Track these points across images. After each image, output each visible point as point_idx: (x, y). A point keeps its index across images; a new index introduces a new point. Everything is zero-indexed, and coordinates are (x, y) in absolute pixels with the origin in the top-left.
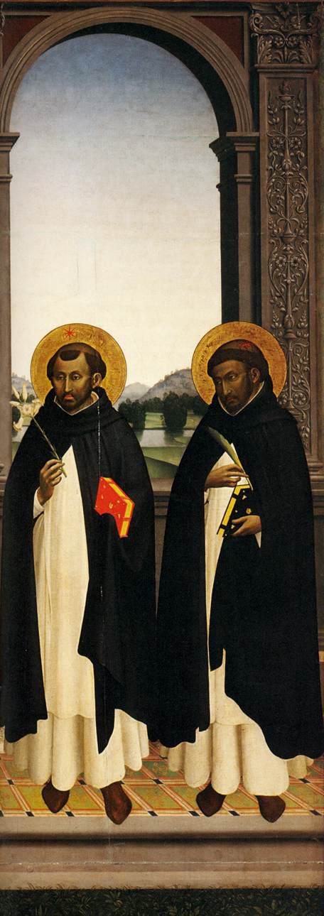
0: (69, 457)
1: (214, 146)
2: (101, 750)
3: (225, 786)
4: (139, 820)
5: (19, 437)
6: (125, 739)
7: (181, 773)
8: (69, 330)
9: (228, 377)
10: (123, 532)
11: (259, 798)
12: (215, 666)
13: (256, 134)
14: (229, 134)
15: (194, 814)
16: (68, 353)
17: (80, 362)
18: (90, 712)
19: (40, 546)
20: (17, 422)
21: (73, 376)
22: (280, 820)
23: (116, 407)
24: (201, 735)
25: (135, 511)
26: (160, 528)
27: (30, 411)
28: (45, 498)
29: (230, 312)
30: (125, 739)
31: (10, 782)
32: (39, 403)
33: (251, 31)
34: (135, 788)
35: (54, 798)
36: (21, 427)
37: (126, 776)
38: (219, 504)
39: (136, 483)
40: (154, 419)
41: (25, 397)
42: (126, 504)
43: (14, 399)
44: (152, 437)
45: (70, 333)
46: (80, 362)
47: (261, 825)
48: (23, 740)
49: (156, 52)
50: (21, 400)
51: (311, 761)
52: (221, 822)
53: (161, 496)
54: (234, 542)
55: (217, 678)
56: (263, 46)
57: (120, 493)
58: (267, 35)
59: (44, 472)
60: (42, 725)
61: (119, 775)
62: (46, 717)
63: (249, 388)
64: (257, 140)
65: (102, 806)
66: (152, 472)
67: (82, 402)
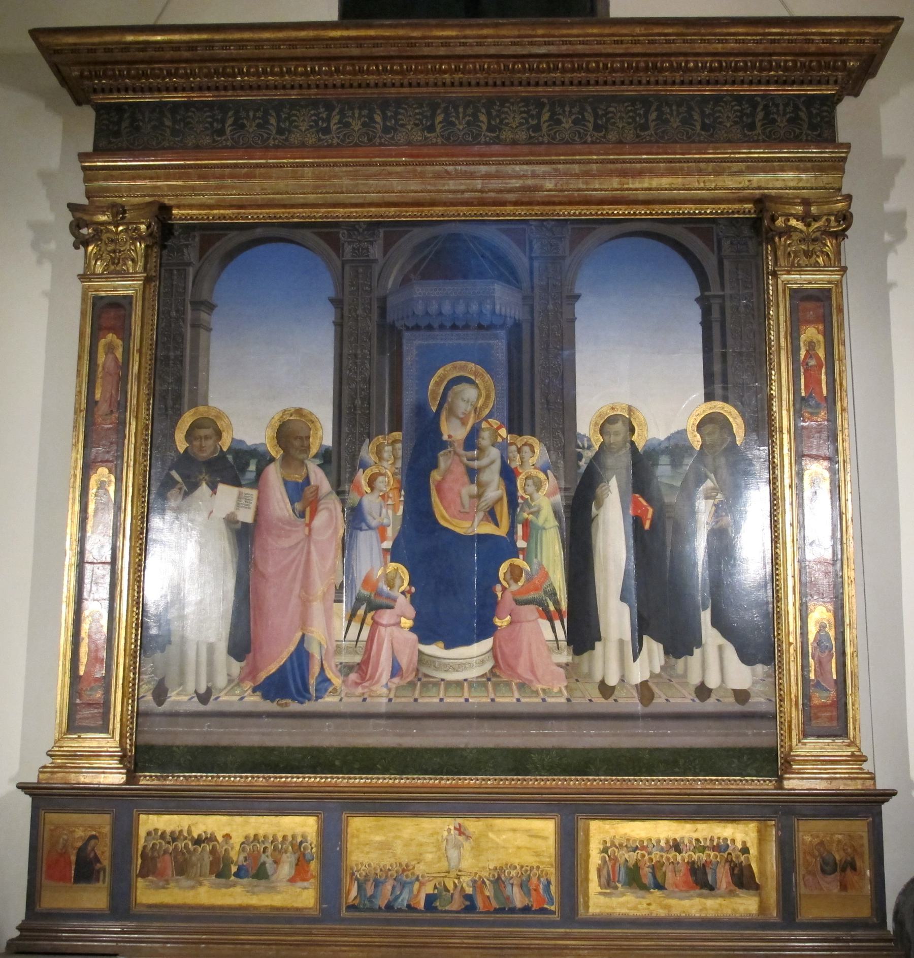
1: (697, 300)
2: (635, 660)
3: (713, 682)
4: (660, 703)
7: (685, 675)
10: (647, 526)
12: (704, 609)
13: (722, 293)
14: (707, 293)
15: (693, 700)
16: (611, 420)
17: (619, 426)
18: (627, 636)
19: (596, 535)
20: (580, 460)
22: (747, 705)
24: (697, 652)
25: (654, 513)
27: (588, 455)
28: (599, 507)
29: (709, 397)
31: (577, 680)
33: (718, 235)
34: (657, 684)
35: (605, 690)
36: (583, 464)
37: (651, 677)
41: (586, 446)
43: (578, 447)
45: (613, 409)
46: (619, 426)
47: (738, 708)
48: (586, 655)
49: (661, 246)
50: (583, 448)
51: (766, 668)
52: (710, 705)
56: (726, 244)
57: (645, 503)
58: (727, 237)
59: (599, 491)
60: (598, 645)
61: (647, 676)
62: (599, 639)
64: (722, 297)
65: (635, 694)
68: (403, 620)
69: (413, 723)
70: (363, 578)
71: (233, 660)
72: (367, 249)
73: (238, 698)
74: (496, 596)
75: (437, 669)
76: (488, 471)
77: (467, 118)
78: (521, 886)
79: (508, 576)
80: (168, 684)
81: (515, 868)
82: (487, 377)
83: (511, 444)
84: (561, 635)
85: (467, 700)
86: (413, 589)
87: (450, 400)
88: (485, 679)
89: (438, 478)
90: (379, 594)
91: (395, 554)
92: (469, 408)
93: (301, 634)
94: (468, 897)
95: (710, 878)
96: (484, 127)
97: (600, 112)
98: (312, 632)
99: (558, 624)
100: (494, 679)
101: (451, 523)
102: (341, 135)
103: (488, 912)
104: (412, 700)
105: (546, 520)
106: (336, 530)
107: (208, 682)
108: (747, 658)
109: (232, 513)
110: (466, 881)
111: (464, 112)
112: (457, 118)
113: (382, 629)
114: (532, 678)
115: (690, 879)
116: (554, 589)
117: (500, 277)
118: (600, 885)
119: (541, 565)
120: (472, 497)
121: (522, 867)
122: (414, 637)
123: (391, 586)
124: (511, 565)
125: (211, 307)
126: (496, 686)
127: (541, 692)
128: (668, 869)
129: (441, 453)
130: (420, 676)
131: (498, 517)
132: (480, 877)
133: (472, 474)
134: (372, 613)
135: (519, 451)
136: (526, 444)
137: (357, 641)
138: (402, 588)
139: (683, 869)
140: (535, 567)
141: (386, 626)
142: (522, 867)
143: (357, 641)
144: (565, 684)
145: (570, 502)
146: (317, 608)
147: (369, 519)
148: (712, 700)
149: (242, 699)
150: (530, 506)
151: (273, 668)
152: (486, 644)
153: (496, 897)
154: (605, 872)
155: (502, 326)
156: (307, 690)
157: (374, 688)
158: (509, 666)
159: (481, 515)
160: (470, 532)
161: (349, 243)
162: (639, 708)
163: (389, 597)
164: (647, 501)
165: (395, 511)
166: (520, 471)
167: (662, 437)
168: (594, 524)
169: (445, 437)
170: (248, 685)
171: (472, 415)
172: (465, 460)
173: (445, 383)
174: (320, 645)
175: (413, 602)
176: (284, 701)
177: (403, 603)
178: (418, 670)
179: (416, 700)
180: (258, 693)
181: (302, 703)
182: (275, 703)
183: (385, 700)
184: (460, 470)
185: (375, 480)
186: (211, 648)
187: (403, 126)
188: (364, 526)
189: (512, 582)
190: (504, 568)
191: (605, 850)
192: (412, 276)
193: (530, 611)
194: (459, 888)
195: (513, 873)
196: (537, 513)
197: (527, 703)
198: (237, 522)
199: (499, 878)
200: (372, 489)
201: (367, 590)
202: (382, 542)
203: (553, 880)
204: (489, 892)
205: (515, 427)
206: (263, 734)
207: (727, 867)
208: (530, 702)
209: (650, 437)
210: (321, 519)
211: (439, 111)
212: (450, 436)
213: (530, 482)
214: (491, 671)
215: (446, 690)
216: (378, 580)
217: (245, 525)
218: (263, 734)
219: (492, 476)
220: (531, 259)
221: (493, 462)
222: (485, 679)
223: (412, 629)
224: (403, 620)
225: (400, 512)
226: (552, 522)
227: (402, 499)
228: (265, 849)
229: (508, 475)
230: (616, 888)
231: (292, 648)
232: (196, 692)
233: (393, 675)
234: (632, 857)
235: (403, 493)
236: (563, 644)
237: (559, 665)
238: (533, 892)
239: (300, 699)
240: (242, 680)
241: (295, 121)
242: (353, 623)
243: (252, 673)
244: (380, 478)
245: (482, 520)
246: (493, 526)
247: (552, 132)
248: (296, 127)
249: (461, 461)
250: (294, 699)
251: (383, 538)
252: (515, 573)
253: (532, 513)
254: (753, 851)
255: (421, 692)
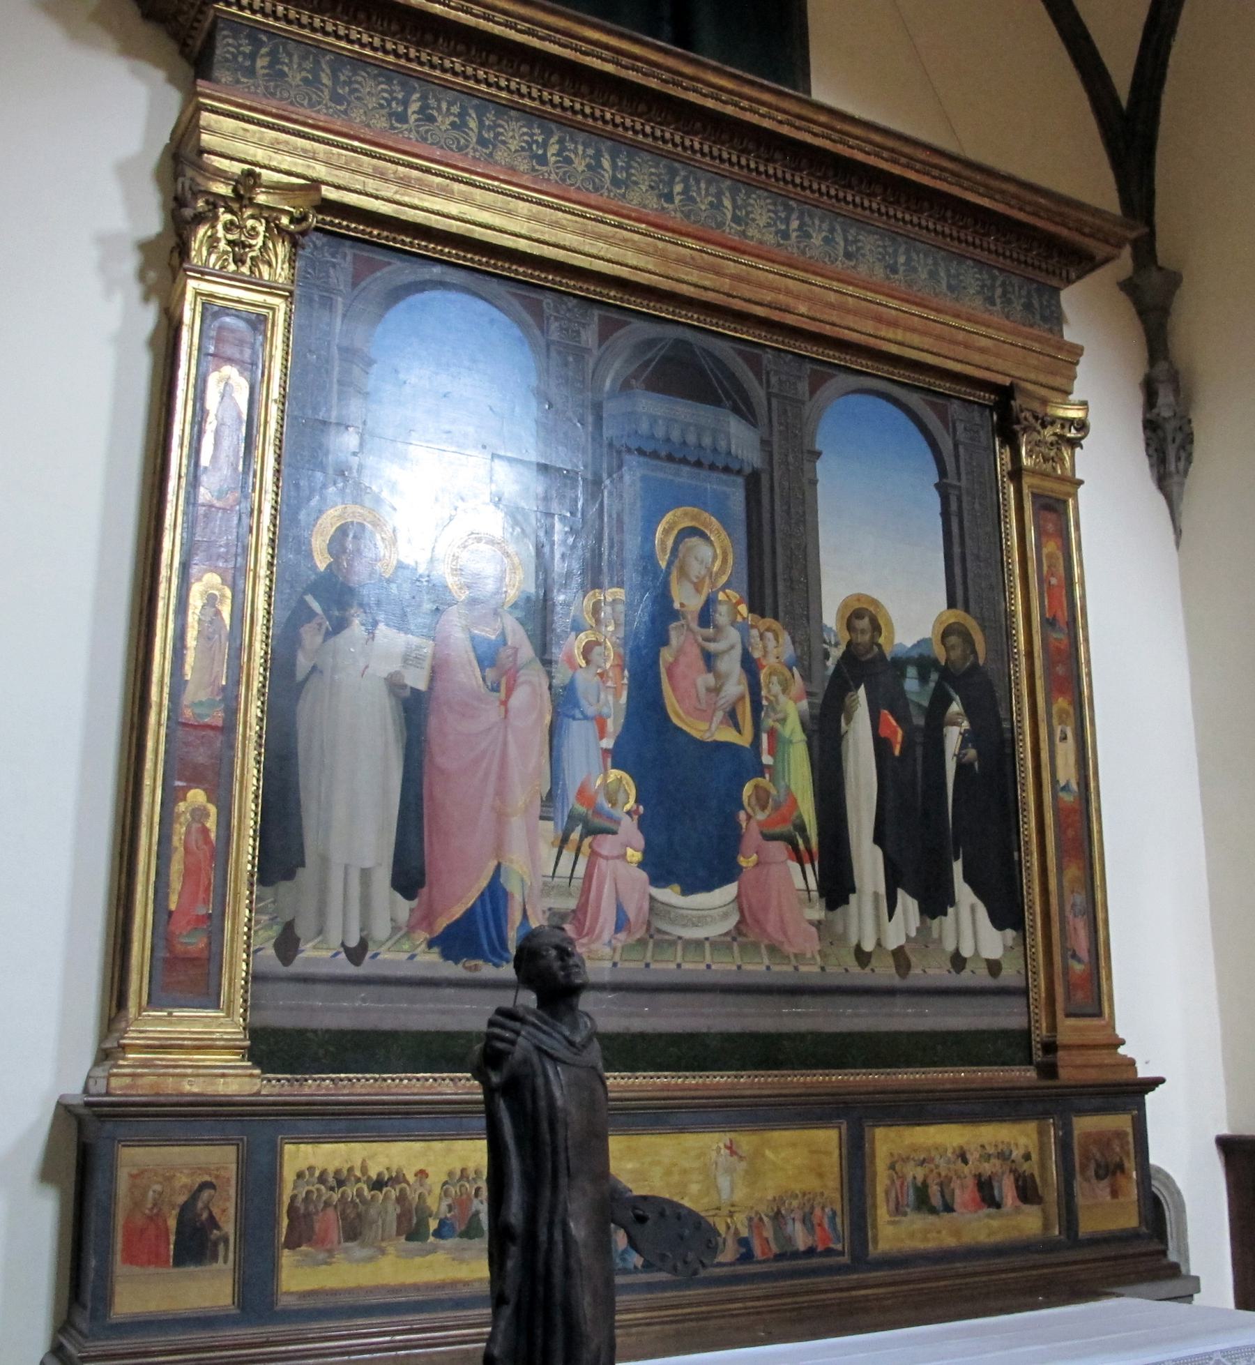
0: (862, 691)
2: (890, 918)
3: (967, 952)
5: (830, 671)
6: (905, 912)
7: (940, 939)
8: (859, 597)
9: (953, 647)
10: (897, 752)
11: (988, 961)
12: (957, 858)
16: (858, 614)
17: (864, 623)
18: (882, 889)
21: (863, 632)
23: (889, 658)
24: (950, 910)
25: (903, 737)
26: (919, 751)
27: (836, 653)
28: (849, 720)
29: (951, 604)
30: (905, 912)
32: (842, 648)
35: (862, 957)
36: (831, 664)
38: (953, 738)
39: (903, 719)
40: (912, 671)
42: (895, 733)
43: (825, 642)
44: (911, 684)
45: (859, 600)
46: (864, 623)
48: (839, 910)
50: (830, 644)
52: (965, 978)
53: (917, 728)
54: (962, 768)
55: (958, 867)
56: (960, 427)
57: (894, 723)
59: (847, 700)
61: (902, 941)
63: (965, 658)
66: (913, 710)
67: (867, 652)
68: (630, 851)
69: (644, 997)
70: (578, 785)
71: (399, 896)
72: (578, 332)
73: (406, 956)
74: (740, 826)
75: (673, 922)
76: (726, 657)
77: (710, 198)
78: (804, 1221)
79: (753, 801)
80: (300, 930)
81: (797, 1196)
82: (724, 534)
83: (752, 627)
84: (813, 884)
85: (709, 967)
86: (641, 808)
87: (681, 555)
88: (729, 939)
89: (671, 659)
90: (598, 812)
91: (617, 758)
92: (703, 572)
93: (495, 863)
94: (744, 1242)
95: (996, 1192)
96: (729, 216)
97: (850, 238)
98: (511, 861)
99: (808, 867)
100: (740, 939)
101: (686, 724)
102: (561, 171)
103: (764, 1261)
104: (642, 965)
105: (793, 732)
106: (541, 716)
107: (362, 930)
108: (999, 922)
109: (397, 673)
110: (740, 1221)
111: (707, 190)
112: (699, 193)
113: (602, 862)
114: (781, 938)
115: (977, 1195)
116: (803, 822)
117: (736, 410)
118: (889, 1212)
119: (788, 788)
120: (709, 690)
121: (804, 1194)
122: (643, 875)
123: (614, 804)
124: (756, 787)
125: (370, 363)
126: (743, 947)
127: (792, 958)
128: (956, 1184)
129: (673, 625)
130: (652, 931)
131: (741, 723)
132: (757, 1213)
133: (709, 659)
134: (588, 840)
135: (762, 636)
136: (768, 630)
137: (571, 877)
138: (628, 807)
139: (970, 1182)
140: (782, 791)
141: (607, 858)
142: (804, 1194)
143: (571, 877)
144: (818, 948)
145: (817, 711)
146: (517, 826)
147: (583, 702)
148: (966, 973)
149: (412, 957)
150: (774, 710)
151: (458, 912)
152: (730, 890)
153: (776, 1239)
154: (893, 1195)
155: (739, 472)
156: (506, 950)
157: (594, 947)
158: (757, 921)
159: (720, 715)
160: (707, 737)
161: (556, 319)
162: (897, 981)
163: (610, 818)
164: (897, 720)
165: (617, 695)
166: (764, 663)
167: (909, 644)
168: (844, 743)
169: (677, 606)
170: (422, 936)
171: (707, 580)
172: (700, 639)
173: (675, 532)
174: (522, 880)
175: (641, 826)
176: (473, 963)
177: (629, 827)
178: (649, 924)
179: (647, 965)
180: (436, 950)
181: (497, 965)
182: (460, 966)
183: (608, 964)
184: (694, 652)
185: (592, 649)
186: (366, 874)
187: (636, 183)
188: (579, 715)
189: (757, 808)
190: (748, 789)
191: (892, 1167)
192: (633, 382)
193: (778, 849)
194: (732, 1230)
195: (795, 1203)
196: (783, 721)
197: (778, 973)
198: (405, 686)
199: (778, 1213)
200: (588, 662)
201: (582, 804)
202: (601, 738)
203: (838, 1208)
204: (768, 1233)
205: (756, 607)
206: (443, 1012)
207: (1012, 1178)
208: (782, 972)
209: (897, 641)
210: (520, 697)
211: (678, 179)
212: (682, 605)
213: (775, 679)
214: (737, 927)
215: (684, 949)
216: (597, 792)
217: (415, 691)
218: (443, 1012)
219: (731, 665)
220: (769, 396)
221: (732, 647)
222: (729, 939)
223: (642, 865)
224: (630, 851)
225: (623, 699)
226: (799, 736)
227: (626, 681)
228: (478, 1190)
229: (750, 666)
230: (905, 1214)
231: (484, 883)
232: (343, 945)
233: (618, 929)
234: (920, 1173)
235: (626, 673)
236: (815, 895)
237: (811, 923)
238: (818, 1229)
239: (496, 961)
240: (411, 928)
241: (502, 134)
242: (565, 852)
243: (427, 918)
244: (597, 649)
245: (721, 723)
246: (735, 733)
247: (802, 245)
248: (504, 143)
249: (696, 641)
250: (487, 960)
251: (602, 734)
252: (762, 798)
253: (777, 720)
254: (1035, 1156)
255: (653, 956)
